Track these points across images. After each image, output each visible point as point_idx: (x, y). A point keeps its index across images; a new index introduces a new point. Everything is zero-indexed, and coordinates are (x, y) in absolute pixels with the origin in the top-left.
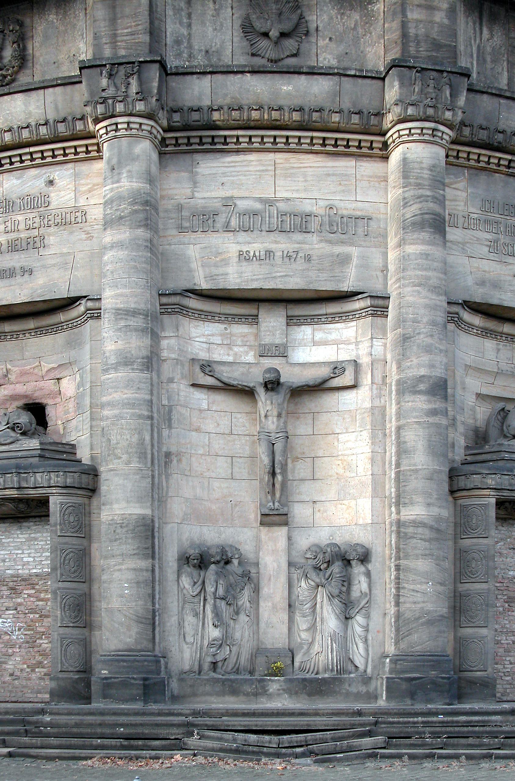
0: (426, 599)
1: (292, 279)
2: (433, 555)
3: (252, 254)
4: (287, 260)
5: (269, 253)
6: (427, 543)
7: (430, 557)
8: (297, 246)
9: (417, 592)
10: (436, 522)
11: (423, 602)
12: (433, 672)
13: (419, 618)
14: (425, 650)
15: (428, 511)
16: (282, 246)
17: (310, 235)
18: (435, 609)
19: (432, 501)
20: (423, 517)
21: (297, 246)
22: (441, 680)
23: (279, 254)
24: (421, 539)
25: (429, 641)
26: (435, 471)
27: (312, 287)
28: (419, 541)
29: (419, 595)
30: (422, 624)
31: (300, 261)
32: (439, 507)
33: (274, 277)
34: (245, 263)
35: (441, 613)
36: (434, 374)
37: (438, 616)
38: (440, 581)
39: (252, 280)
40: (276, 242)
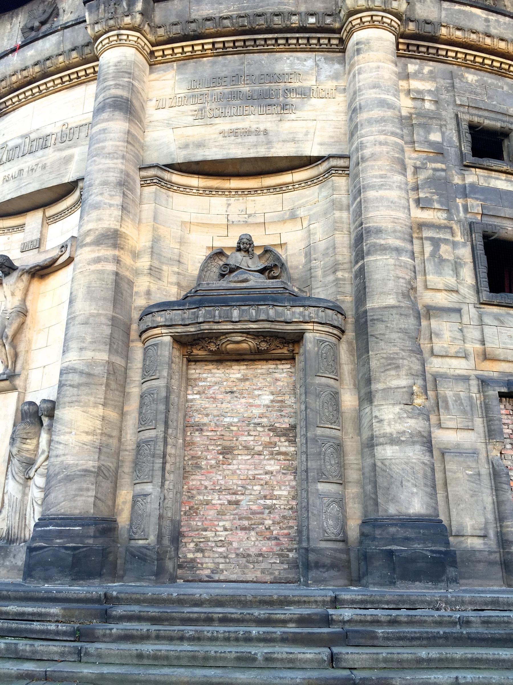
0: (67, 452)
1: (31, 185)
2: (79, 402)
3: (10, 176)
4: (30, 172)
5: (21, 170)
6: (75, 389)
7: (77, 404)
8: (39, 160)
9: (60, 443)
10: (88, 366)
11: (64, 455)
12: (58, 541)
13: (58, 473)
14: (59, 513)
15: (80, 356)
16: (28, 164)
17: (47, 149)
18: (76, 462)
19: (84, 345)
20: (75, 362)
21: (39, 160)
22: (64, 551)
23: (26, 170)
24: (70, 386)
25: (64, 501)
26: (92, 315)
27: (44, 187)
28: (68, 388)
29: (61, 447)
30: (60, 481)
31: (39, 170)
32: (94, 350)
33: (21, 188)
34: (5, 184)
35: (84, 467)
36: (100, 226)
37: (79, 471)
38: (87, 430)
39: (8, 194)
40: (26, 162)
